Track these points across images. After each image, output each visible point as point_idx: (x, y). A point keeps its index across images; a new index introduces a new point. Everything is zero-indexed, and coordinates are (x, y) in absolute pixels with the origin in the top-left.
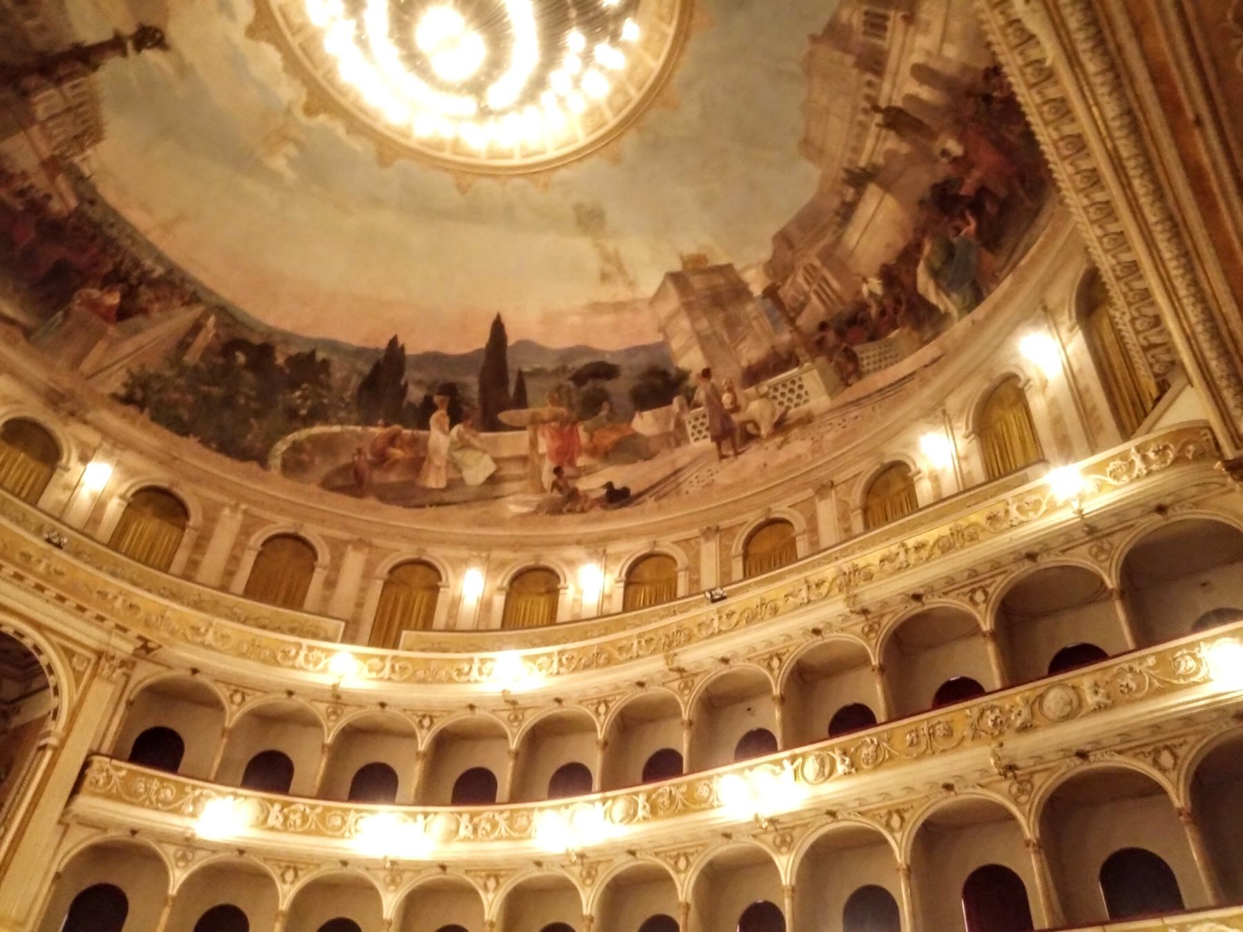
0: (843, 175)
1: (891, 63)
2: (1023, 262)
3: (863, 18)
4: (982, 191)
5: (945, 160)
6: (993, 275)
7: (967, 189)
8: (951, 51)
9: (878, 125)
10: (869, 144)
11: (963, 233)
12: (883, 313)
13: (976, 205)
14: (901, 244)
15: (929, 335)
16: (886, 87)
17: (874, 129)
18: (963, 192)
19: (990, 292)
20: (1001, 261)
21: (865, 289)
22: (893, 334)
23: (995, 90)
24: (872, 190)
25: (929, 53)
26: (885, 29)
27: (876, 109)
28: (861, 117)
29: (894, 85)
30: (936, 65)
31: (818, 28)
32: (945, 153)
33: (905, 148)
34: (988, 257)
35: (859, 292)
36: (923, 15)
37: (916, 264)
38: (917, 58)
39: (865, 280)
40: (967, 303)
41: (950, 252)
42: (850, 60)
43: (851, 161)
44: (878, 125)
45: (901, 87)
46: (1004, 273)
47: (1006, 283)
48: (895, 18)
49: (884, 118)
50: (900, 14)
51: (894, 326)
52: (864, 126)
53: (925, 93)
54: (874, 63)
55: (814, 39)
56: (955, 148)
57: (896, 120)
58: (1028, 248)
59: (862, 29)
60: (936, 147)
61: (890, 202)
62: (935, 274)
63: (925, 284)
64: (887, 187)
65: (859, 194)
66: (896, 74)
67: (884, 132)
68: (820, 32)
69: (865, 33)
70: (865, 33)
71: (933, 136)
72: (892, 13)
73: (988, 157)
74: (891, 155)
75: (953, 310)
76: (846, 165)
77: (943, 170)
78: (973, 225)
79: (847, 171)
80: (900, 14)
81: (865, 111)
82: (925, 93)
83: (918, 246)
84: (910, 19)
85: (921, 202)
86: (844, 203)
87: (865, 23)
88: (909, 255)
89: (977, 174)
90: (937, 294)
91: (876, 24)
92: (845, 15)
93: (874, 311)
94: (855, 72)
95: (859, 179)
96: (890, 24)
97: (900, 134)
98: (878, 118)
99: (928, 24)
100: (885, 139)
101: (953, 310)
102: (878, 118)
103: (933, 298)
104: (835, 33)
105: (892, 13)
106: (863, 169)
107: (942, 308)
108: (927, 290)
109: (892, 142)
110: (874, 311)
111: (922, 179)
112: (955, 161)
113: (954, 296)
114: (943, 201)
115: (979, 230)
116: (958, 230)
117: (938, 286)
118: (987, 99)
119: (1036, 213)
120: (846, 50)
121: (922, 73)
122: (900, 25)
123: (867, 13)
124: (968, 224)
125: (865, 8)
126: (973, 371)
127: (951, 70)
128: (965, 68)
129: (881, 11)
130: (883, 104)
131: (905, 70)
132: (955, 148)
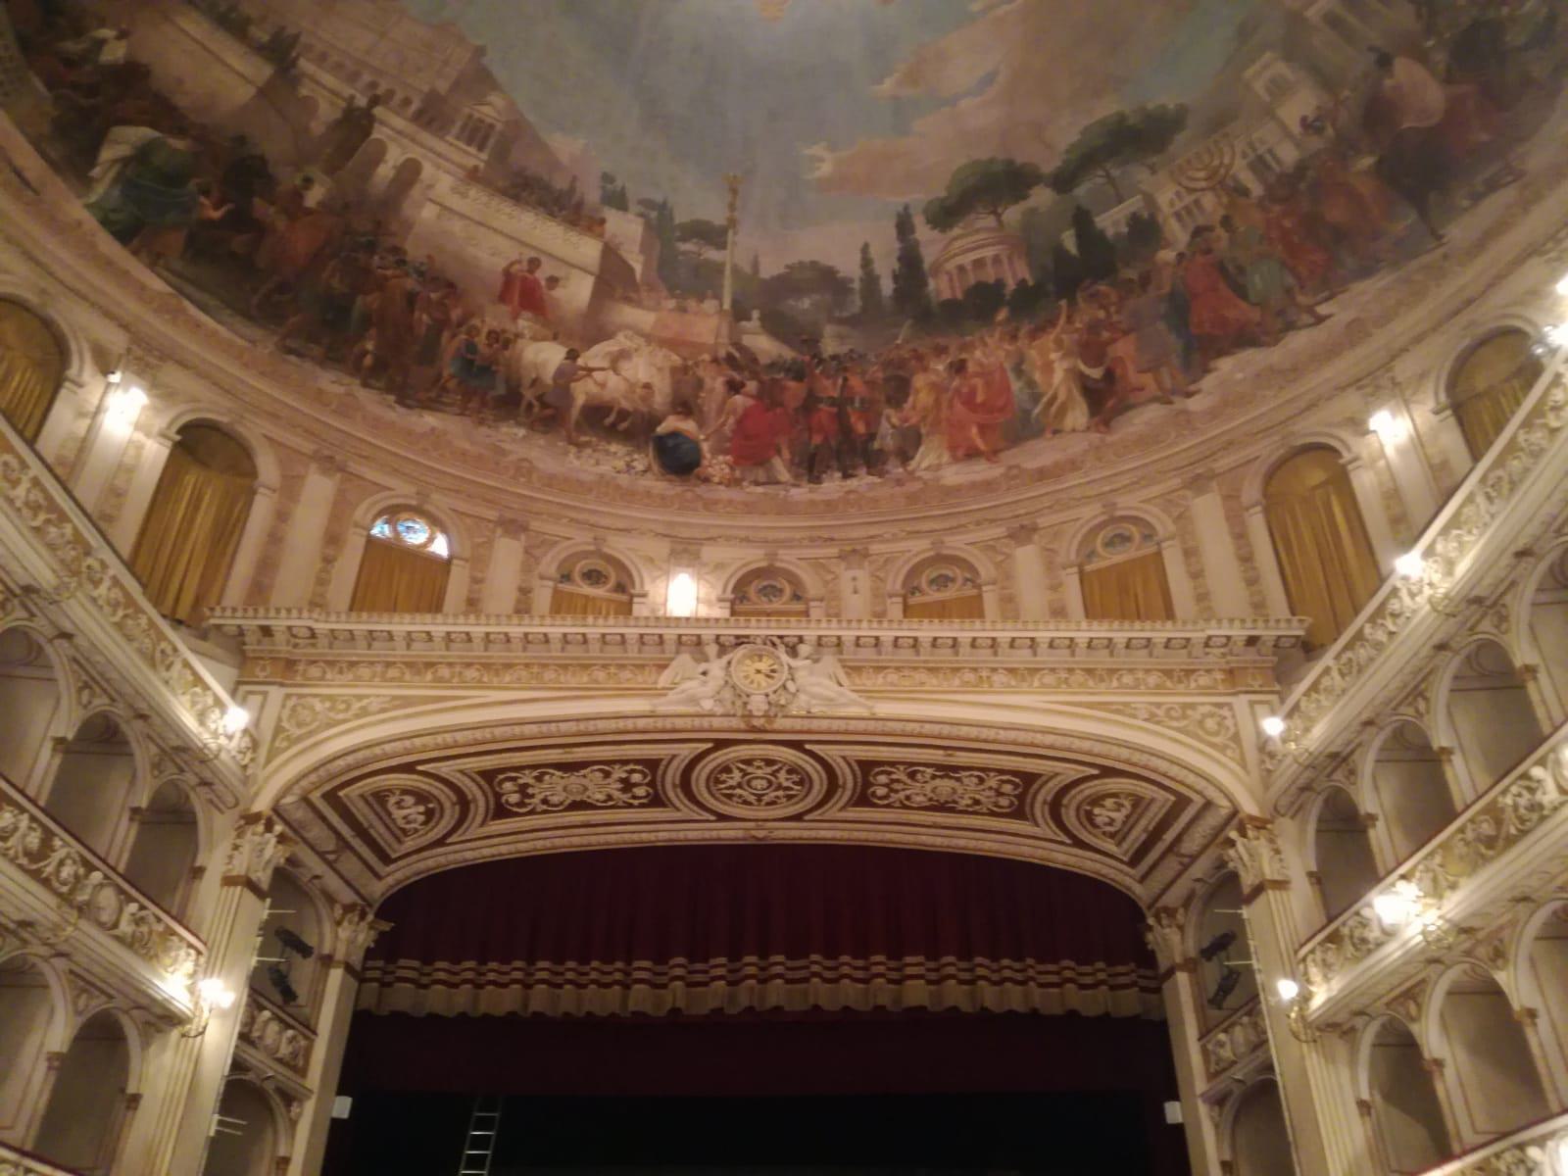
0: (291, 31)
1: (426, 137)
2: (187, 303)
3: (489, 120)
4: (260, 230)
5: (298, 181)
6: (159, 255)
7: (261, 208)
8: (428, 212)
9: (352, 98)
10: (328, 79)
11: (203, 199)
12: (70, 63)
13: (241, 220)
14: (181, 101)
15: (53, 155)
16: (399, 123)
17: (347, 91)
18: (257, 201)
19: (135, 253)
20: (178, 265)
21: (106, 33)
22: (38, 84)
23: (382, 258)
24: (264, 71)
25: (430, 187)
26: (469, 143)
27: (375, 101)
28: (367, 78)
29: (400, 133)
30: (416, 192)
31: (492, 61)
32: (308, 182)
33: (317, 127)
34: (176, 240)
35: (102, 24)
36: (473, 192)
37: (152, 125)
38: (428, 170)
39: (123, 35)
40: (113, 217)
41: (174, 179)
42: (443, 86)
43: (309, 48)
44: (352, 98)
45: (396, 143)
46: (165, 273)
47: (157, 284)
48: (477, 159)
49: (358, 109)
50: (482, 165)
51: (50, 85)
52: (353, 78)
53: (385, 171)
54: (431, 115)
55: (480, 51)
56: (314, 197)
57: (356, 124)
58: (203, 308)
59: (477, 115)
60: (314, 171)
61: (244, 93)
62: (142, 154)
63: (124, 141)
64: (263, 93)
65: (260, 49)
66: (413, 140)
67: (343, 104)
68: (485, 61)
69: (470, 116)
70: (470, 116)
71: (331, 170)
72: (484, 156)
73: (301, 241)
74: (309, 106)
75: (99, 191)
76: (303, 39)
77: (288, 179)
78: (216, 215)
79: (296, 37)
80: (482, 165)
81: (373, 85)
82: (385, 171)
83: (181, 131)
84: (473, 176)
85: (241, 140)
86: (248, 21)
87: (482, 121)
88: (164, 113)
89: (281, 223)
90: (115, 161)
91: (476, 134)
92: (496, 99)
93: (71, 46)
94: (426, 88)
95: (281, 52)
96: (472, 150)
97: (338, 124)
98: (362, 101)
99: (464, 195)
100: (332, 104)
101: (99, 191)
102: (362, 101)
103: (107, 154)
104: (479, 79)
105: (484, 156)
106: (294, 63)
107: (96, 172)
108: (117, 143)
109: (328, 111)
110: (71, 46)
111: (273, 145)
112: (298, 195)
113: (116, 193)
114: (243, 173)
115: (211, 222)
116: (206, 193)
117: (125, 161)
118: (371, 248)
119: (247, 316)
120: (456, 85)
121: (409, 173)
122: (471, 162)
123: (492, 126)
124: (216, 208)
125: (499, 127)
126: (38, 263)
127: (407, 209)
128: (408, 226)
129: (491, 142)
130: (378, 111)
131: (415, 153)
132: (314, 197)
